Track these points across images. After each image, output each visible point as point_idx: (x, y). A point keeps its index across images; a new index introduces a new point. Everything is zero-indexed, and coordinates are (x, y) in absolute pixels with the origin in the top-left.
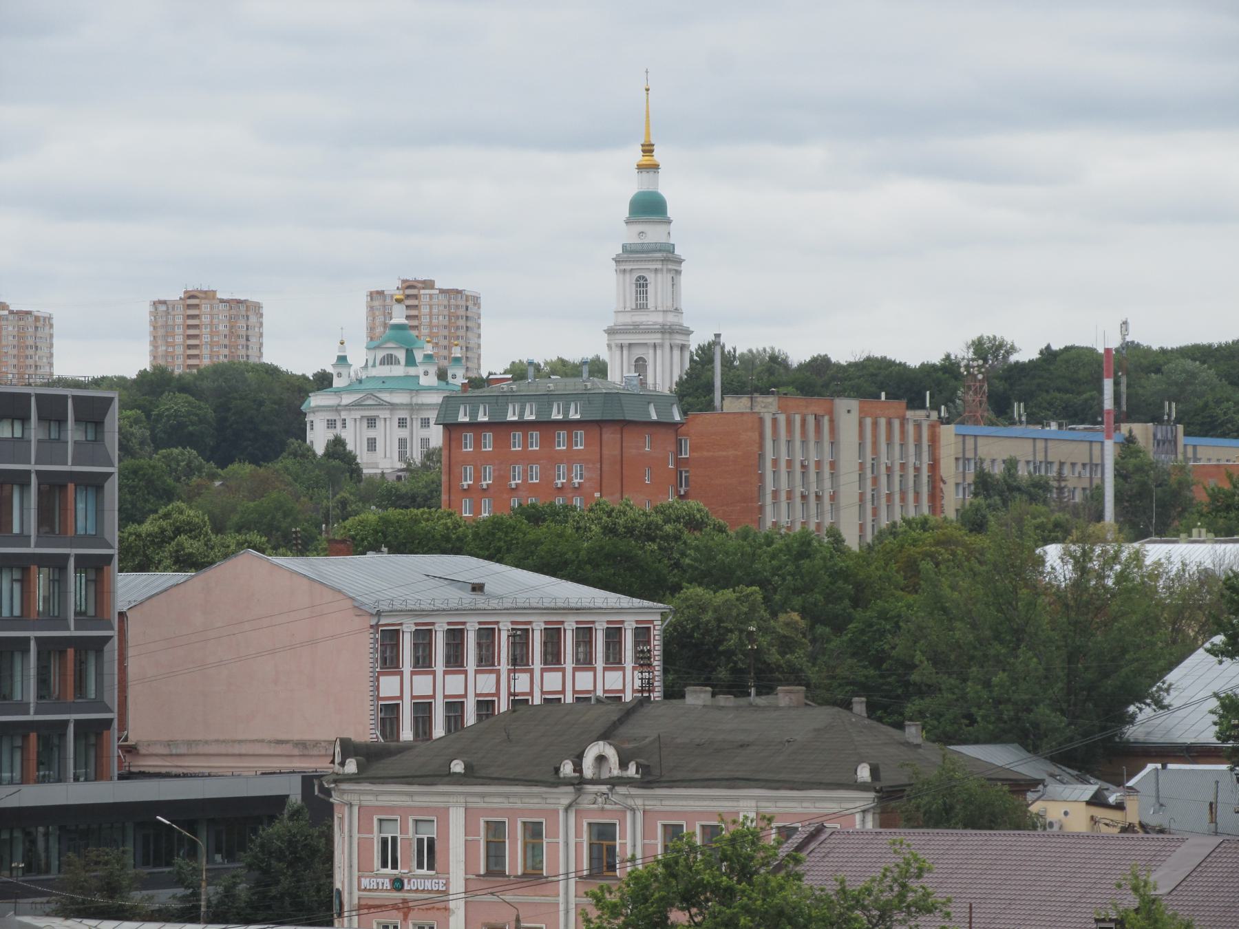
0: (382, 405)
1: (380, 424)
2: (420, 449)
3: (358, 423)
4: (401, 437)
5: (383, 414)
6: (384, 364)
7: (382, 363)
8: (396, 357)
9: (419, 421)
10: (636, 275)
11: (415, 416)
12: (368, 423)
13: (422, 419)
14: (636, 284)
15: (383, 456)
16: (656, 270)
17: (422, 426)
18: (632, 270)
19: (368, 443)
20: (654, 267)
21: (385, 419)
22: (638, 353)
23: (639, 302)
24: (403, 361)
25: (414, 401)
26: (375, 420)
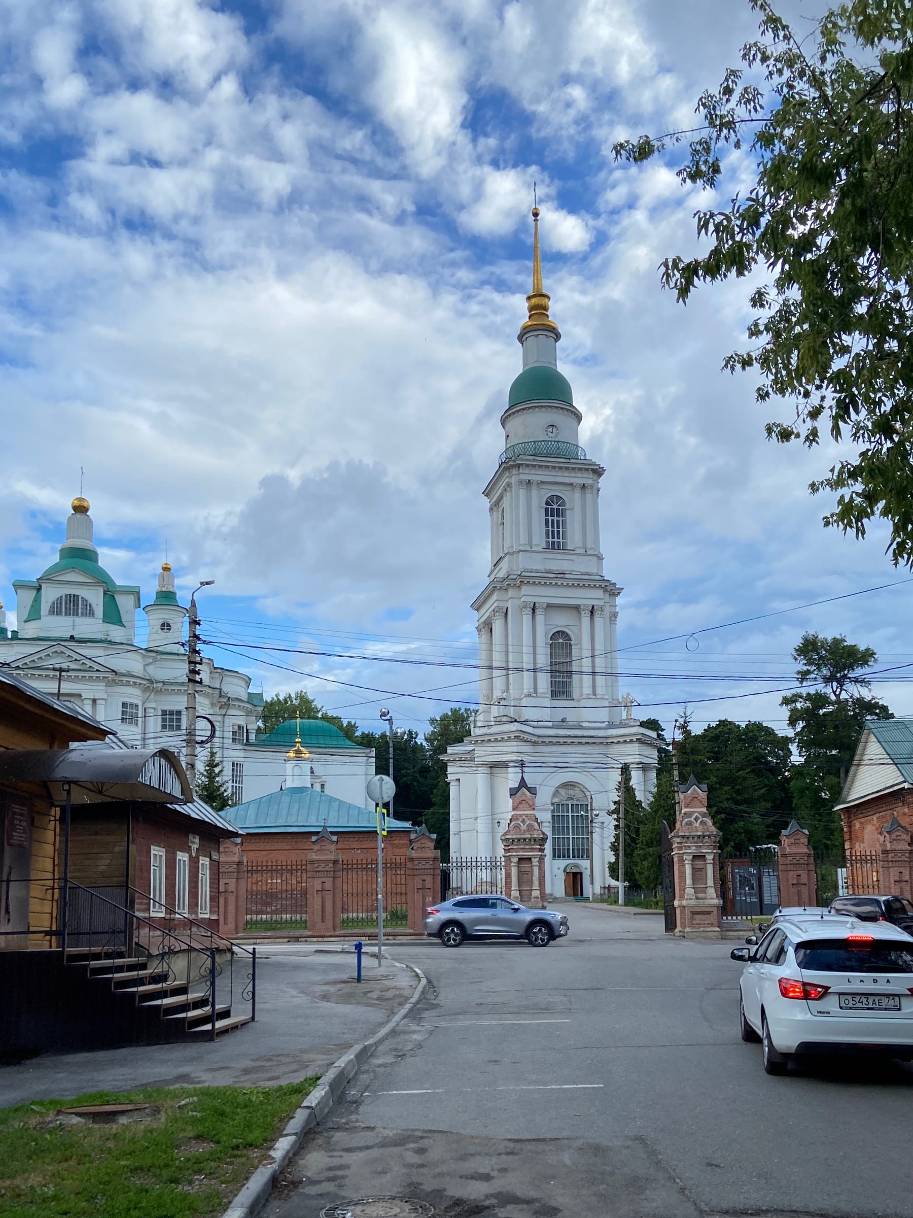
6: (59, 613)
7: (55, 610)
10: (547, 493)
13: (164, 713)
14: (546, 510)
16: (583, 487)
18: (542, 482)
20: (582, 481)
21: (94, 701)
22: (561, 621)
23: (556, 540)
24: (99, 611)
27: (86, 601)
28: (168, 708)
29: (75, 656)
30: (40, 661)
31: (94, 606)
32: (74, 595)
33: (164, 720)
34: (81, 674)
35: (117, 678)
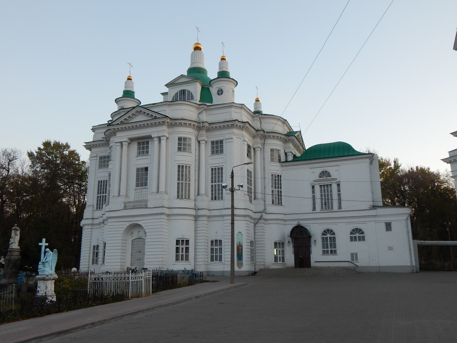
0: (156, 118)
1: (154, 146)
2: (210, 184)
3: (125, 147)
4: (182, 163)
5: (153, 132)
8: (189, 92)
12: (139, 148)
13: (213, 143)
15: (155, 190)
17: (213, 153)
19: (138, 175)
21: (159, 138)
25: (205, 117)
26: (148, 143)
27: (189, 92)
28: (215, 139)
29: (151, 113)
30: (130, 119)
31: (193, 94)
32: (183, 90)
33: (213, 148)
34: (149, 122)
35: (173, 122)
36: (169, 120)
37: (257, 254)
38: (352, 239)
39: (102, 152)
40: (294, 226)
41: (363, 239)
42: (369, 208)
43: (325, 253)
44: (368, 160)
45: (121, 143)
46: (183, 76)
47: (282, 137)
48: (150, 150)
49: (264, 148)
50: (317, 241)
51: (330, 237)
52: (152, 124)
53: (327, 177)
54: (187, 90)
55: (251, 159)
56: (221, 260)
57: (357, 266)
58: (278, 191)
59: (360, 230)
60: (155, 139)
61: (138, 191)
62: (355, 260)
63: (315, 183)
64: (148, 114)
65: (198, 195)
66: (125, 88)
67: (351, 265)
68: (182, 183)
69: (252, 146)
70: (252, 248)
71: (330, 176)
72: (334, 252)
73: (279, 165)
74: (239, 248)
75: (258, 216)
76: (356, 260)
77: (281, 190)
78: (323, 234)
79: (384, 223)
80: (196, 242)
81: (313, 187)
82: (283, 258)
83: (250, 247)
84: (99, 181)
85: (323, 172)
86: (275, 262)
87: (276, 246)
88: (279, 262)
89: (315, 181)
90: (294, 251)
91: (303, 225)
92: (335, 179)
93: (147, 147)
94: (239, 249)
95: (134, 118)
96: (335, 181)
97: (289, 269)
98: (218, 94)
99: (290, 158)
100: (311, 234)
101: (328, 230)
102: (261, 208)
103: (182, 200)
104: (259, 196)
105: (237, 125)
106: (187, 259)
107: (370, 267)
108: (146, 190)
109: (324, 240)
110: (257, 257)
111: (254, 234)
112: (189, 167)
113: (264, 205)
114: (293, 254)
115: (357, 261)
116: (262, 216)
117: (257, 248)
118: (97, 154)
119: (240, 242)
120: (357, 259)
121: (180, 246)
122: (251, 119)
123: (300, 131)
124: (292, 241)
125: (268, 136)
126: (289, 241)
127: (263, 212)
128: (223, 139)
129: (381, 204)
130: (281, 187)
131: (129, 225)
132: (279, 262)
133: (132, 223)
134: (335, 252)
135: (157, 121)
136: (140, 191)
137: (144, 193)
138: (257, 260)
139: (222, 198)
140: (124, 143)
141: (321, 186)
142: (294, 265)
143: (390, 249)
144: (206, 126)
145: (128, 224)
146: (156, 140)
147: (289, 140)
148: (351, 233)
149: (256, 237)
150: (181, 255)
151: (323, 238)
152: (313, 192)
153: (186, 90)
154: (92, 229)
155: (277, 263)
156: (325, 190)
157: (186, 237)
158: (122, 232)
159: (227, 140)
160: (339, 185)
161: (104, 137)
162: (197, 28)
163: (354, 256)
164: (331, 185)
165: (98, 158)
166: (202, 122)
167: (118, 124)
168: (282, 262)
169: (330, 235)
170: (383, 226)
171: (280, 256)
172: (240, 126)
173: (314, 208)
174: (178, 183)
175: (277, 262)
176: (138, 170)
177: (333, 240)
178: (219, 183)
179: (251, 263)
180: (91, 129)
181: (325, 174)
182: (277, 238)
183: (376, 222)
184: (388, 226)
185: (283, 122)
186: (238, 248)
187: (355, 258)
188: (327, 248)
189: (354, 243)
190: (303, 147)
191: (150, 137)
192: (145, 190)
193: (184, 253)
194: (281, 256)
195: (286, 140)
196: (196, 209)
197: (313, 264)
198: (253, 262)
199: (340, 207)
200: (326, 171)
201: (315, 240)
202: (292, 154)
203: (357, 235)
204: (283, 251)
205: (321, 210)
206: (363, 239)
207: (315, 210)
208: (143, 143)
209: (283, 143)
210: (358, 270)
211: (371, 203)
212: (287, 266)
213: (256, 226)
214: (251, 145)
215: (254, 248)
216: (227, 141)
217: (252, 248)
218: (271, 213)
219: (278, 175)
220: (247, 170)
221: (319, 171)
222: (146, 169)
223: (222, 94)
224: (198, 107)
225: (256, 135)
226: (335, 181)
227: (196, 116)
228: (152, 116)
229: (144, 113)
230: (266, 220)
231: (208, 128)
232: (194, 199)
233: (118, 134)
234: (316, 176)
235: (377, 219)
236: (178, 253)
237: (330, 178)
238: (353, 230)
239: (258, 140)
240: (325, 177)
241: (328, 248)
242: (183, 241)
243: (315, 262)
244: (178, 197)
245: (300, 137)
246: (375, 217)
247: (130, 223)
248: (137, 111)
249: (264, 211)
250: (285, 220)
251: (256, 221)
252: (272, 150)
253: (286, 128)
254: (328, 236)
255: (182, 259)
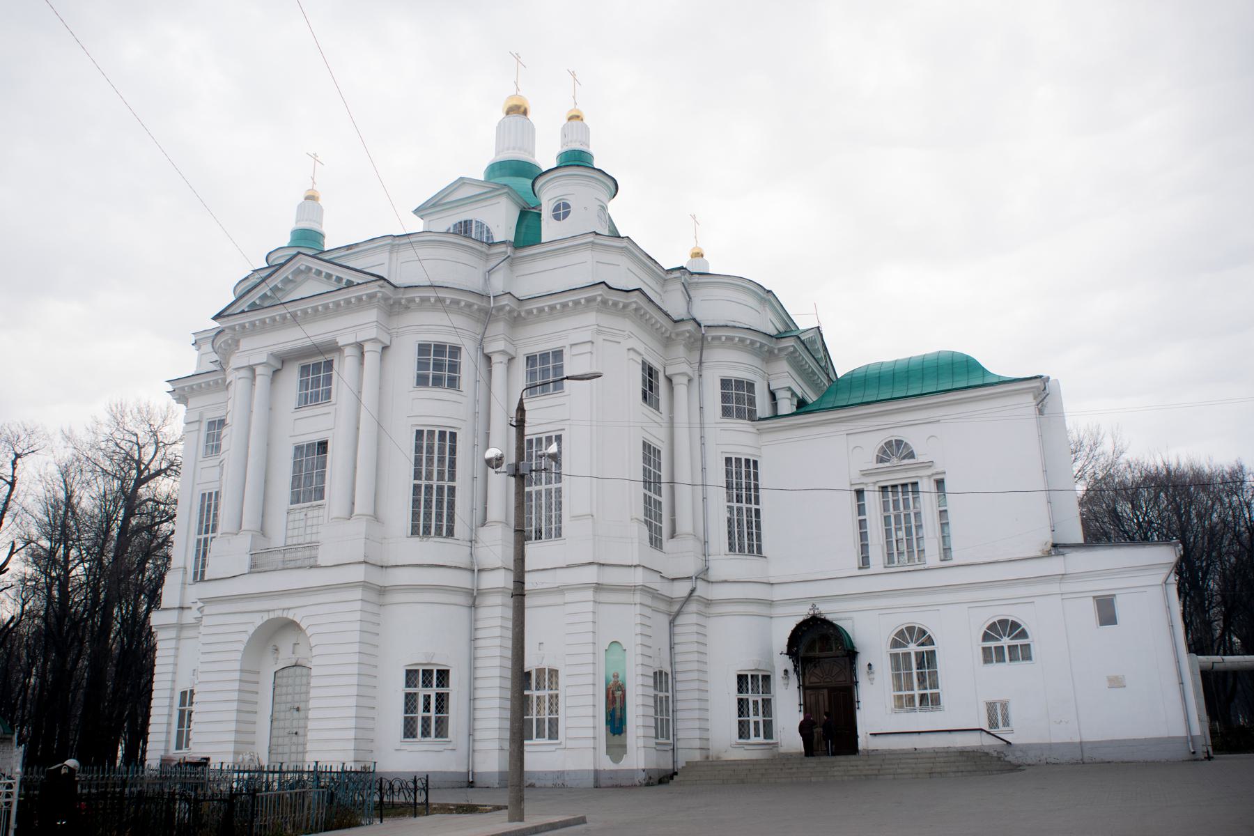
0: (350, 284)
8: (481, 225)
9: (521, 367)
11: (500, 345)
12: (304, 385)
13: (531, 359)
19: (297, 465)
21: (360, 346)
26: (329, 365)
27: (482, 225)
28: (537, 348)
32: (465, 222)
34: (330, 300)
36: (388, 290)
37: (680, 715)
38: (987, 656)
39: (209, 406)
40: (801, 619)
41: (1025, 653)
42: (1039, 554)
43: (904, 703)
44: (1029, 401)
45: (252, 369)
46: (465, 181)
47: (756, 341)
48: (334, 386)
49: (700, 376)
50: (874, 668)
51: (917, 653)
52: (337, 304)
53: (904, 458)
54: (477, 222)
55: (657, 409)
56: (554, 734)
57: (1009, 743)
58: (749, 510)
59: (1015, 625)
60: (348, 351)
61: (297, 517)
62: (1000, 724)
63: (865, 480)
64: (329, 276)
65: (483, 525)
66: (296, 223)
67: (988, 741)
68: (429, 488)
69: (662, 370)
70: (663, 694)
71: (911, 455)
72: (930, 701)
73: (751, 429)
74: (613, 694)
75: (681, 590)
76: (1004, 725)
77: (757, 507)
78: (895, 644)
79: (1092, 598)
80: (473, 679)
81: (860, 493)
82: (768, 725)
83: (652, 692)
84: (204, 495)
85: (889, 444)
86: (740, 737)
87: (744, 686)
88: (753, 739)
89: (866, 474)
90: (802, 703)
91: (829, 617)
92: (930, 464)
93: (329, 380)
94: (614, 698)
95: (291, 291)
96: (929, 472)
97: (783, 761)
98: (557, 217)
99: (786, 406)
100: (855, 645)
101: (911, 630)
102: (690, 566)
103: (425, 539)
104: (684, 525)
105: (604, 302)
106: (442, 730)
107: (1051, 746)
108: (321, 511)
109: (899, 662)
110: (680, 725)
111: (671, 648)
112: (453, 435)
113: (705, 555)
114: (800, 711)
115: (1007, 728)
116: (693, 590)
117: (679, 696)
118: (201, 415)
119: (616, 676)
120: (1006, 723)
121: (421, 691)
122: (657, 288)
123: (818, 328)
124: (795, 670)
125: (714, 338)
126: (786, 671)
127: (696, 578)
128: (564, 347)
129: (1079, 538)
130: (757, 498)
131: (261, 623)
132: (753, 739)
133: (272, 615)
134: (936, 700)
135: (352, 293)
136: (302, 516)
137: (315, 521)
138: (681, 735)
139: (559, 534)
140: (259, 370)
141: (884, 489)
142: (803, 750)
143: (1116, 683)
144: (508, 308)
145: (259, 620)
146: (350, 355)
147: (780, 350)
148: (986, 637)
149: (678, 658)
150: (423, 718)
151: (895, 657)
152: (861, 510)
153: (472, 221)
154: (178, 639)
155: (749, 741)
156: (896, 502)
157: (439, 661)
158: (241, 647)
159: (573, 347)
160: (940, 483)
161: (217, 361)
162: (516, 56)
163: (997, 714)
164: (915, 484)
165: (204, 426)
166: (494, 297)
167: (243, 312)
168: (765, 738)
169: (918, 645)
170: (1090, 612)
171: (756, 719)
172: (615, 304)
173: (865, 562)
174: (417, 488)
175: (749, 738)
176: (299, 449)
177: (927, 660)
178: (549, 486)
179: (657, 744)
180: (193, 344)
181: (895, 450)
182: (747, 664)
183: (1064, 596)
184: (1106, 612)
185: (762, 298)
186: (611, 696)
187: (1000, 718)
188: (908, 690)
189: (996, 667)
190: (828, 375)
191: (335, 348)
192: (316, 513)
193: (432, 713)
194: (760, 718)
195: (771, 352)
196: (475, 570)
197: (864, 741)
198: (668, 738)
199: (946, 552)
200: (899, 442)
201: (870, 665)
202: (794, 394)
203: (1006, 642)
204: (767, 703)
205: (885, 567)
206: (1025, 653)
207: (869, 567)
208: (317, 367)
209: (763, 360)
210: (1010, 758)
211: (1048, 538)
212: (782, 750)
213: (678, 622)
214: (656, 365)
215: (670, 694)
216: (576, 350)
217: (663, 694)
218: (726, 581)
219: (747, 461)
220: (644, 442)
221: (879, 440)
222: (323, 446)
223: (566, 215)
224: (483, 249)
225: (673, 336)
226: (929, 472)
227: (481, 281)
228: (339, 279)
229: (319, 273)
230: (708, 603)
231: (515, 314)
232: (468, 538)
233: (245, 344)
234: (866, 455)
235: (1068, 587)
236: (412, 712)
237: (912, 461)
238: (992, 627)
239: (680, 351)
240: (895, 461)
241: (912, 690)
242: (428, 674)
243: (871, 734)
244: (415, 531)
245: (819, 345)
246: (1061, 579)
247: (266, 617)
248: (298, 268)
249: (703, 575)
250: (770, 603)
251: (676, 608)
252: (725, 383)
253: (770, 315)
254: (913, 648)
255: (426, 733)
